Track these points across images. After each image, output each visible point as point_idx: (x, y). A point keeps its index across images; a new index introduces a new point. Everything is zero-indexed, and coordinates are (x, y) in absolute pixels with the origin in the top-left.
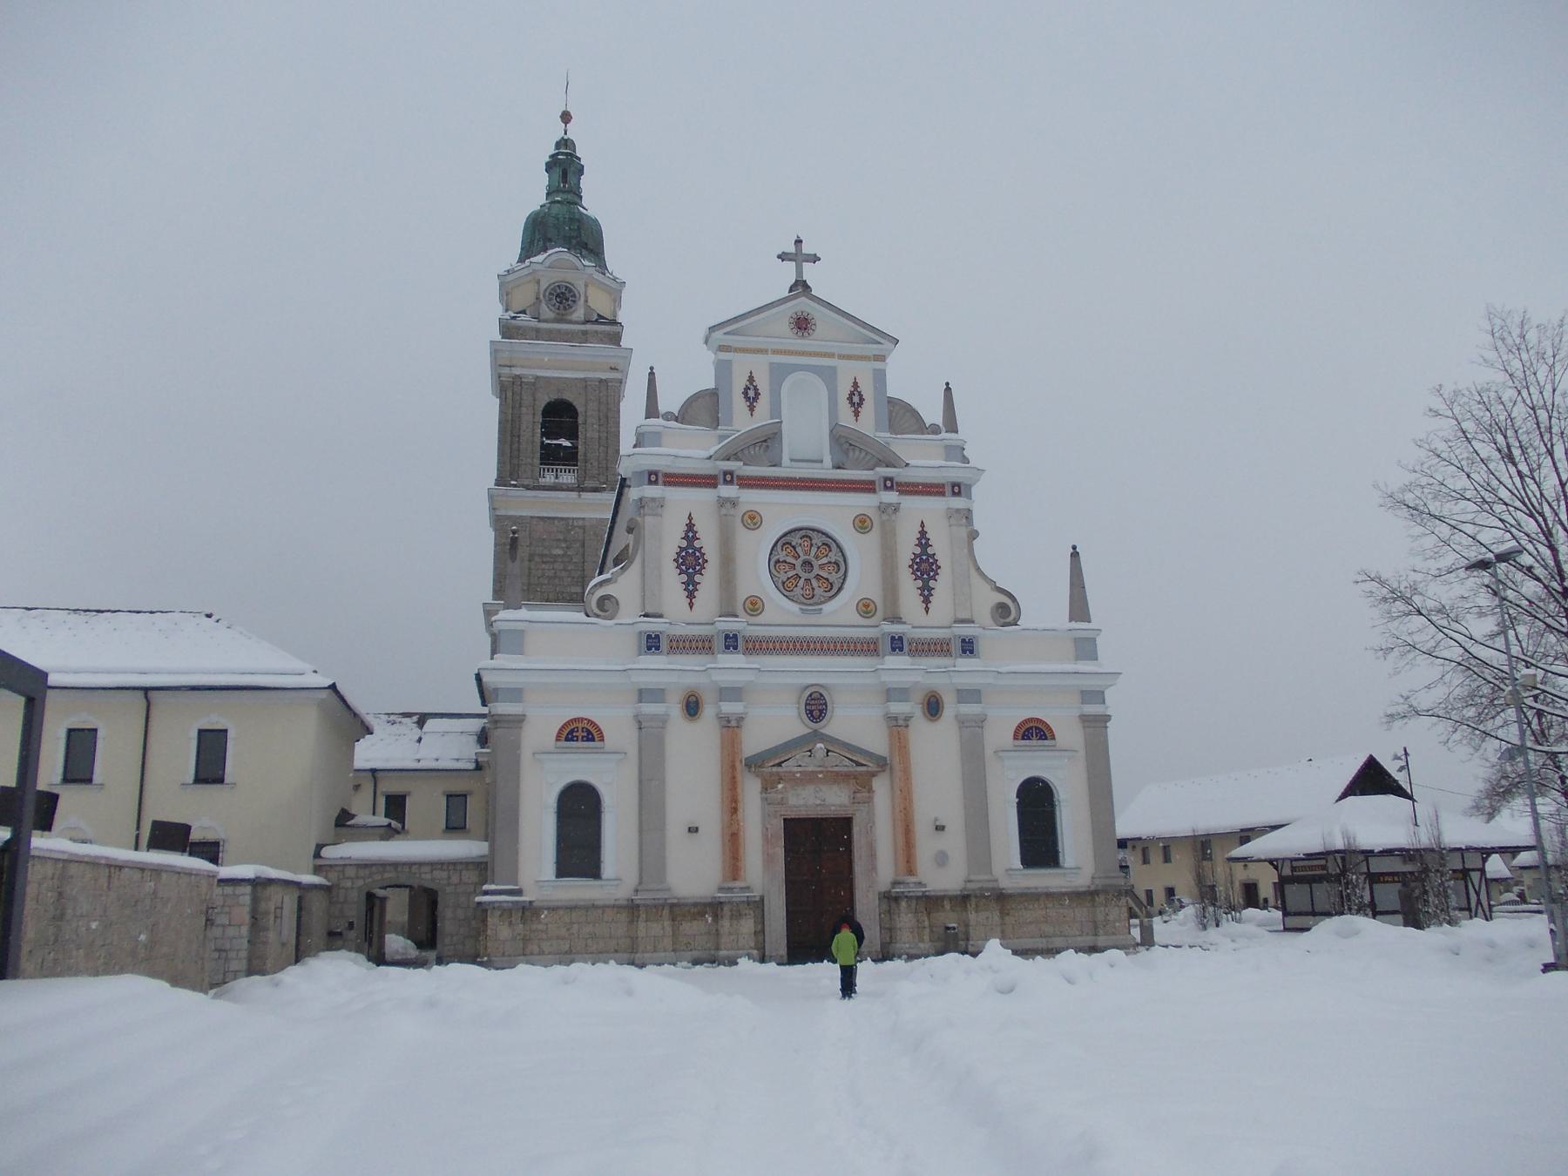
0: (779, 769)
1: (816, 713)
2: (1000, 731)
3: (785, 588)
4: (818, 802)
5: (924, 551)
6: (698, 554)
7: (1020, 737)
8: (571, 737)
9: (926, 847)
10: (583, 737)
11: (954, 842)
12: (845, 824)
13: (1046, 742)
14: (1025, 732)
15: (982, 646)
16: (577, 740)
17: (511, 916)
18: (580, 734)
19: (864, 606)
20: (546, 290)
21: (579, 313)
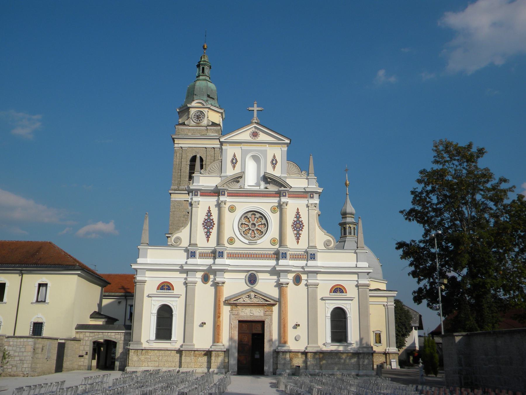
1: (252, 281)
2: (323, 290)
3: (244, 234)
4: (252, 315)
5: (298, 220)
6: (211, 221)
7: (333, 292)
9: (291, 334)
10: (167, 288)
11: (302, 331)
12: (262, 323)
13: (343, 294)
14: (334, 290)
15: (319, 255)
16: (164, 290)
17: (138, 353)
18: (166, 287)
19: (273, 241)
20: (193, 114)
21: (205, 122)
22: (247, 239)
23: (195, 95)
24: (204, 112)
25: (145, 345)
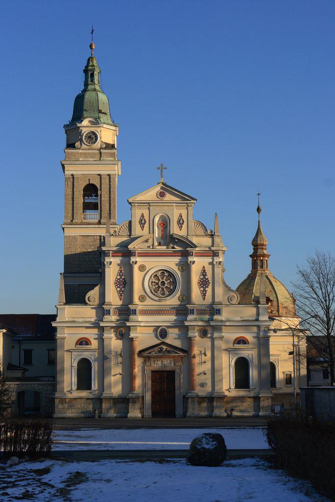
0: (149, 355)
1: (163, 336)
8: (81, 344)
22: (156, 296)
23: (85, 110)
24: (96, 132)
25: (69, 396)
